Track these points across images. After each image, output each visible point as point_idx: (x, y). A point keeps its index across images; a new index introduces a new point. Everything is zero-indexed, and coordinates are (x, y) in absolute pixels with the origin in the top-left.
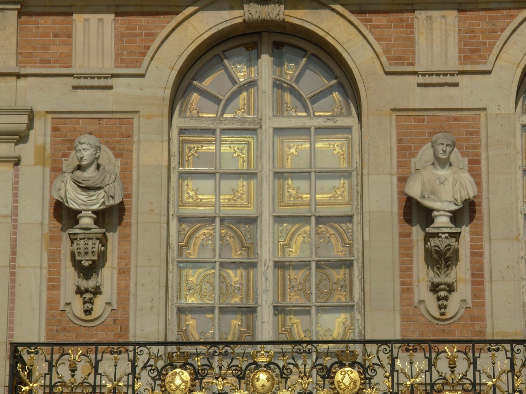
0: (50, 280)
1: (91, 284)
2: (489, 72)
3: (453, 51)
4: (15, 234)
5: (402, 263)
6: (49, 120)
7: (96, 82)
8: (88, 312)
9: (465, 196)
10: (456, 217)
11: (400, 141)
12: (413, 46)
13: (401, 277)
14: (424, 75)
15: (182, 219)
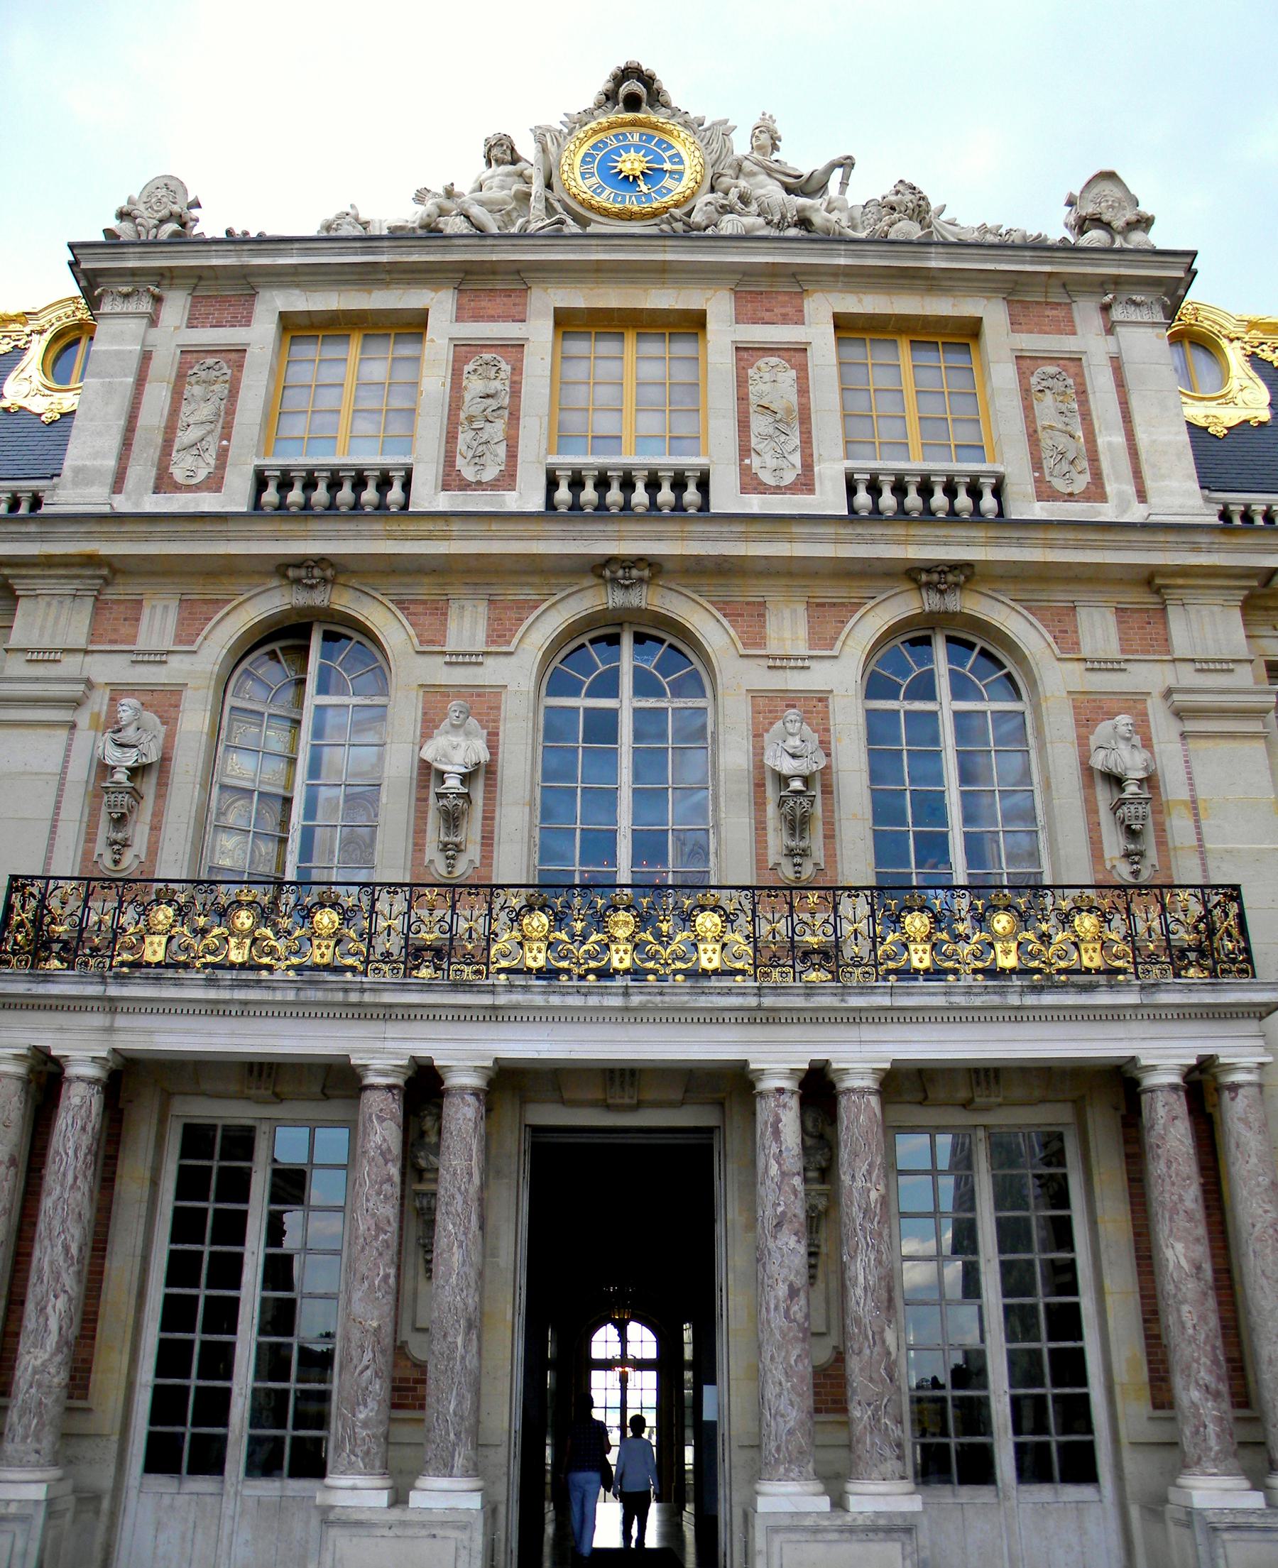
0: (88, 833)
1: (120, 836)
2: (510, 654)
3: (481, 635)
4: (62, 790)
5: (416, 825)
6: (108, 692)
7: (152, 658)
8: (116, 862)
9: (474, 760)
10: (466, 778)
11: (425, 714)
12: (445, 631)
13: (414, 838)
14: (451, 655)
15: (223, 787)
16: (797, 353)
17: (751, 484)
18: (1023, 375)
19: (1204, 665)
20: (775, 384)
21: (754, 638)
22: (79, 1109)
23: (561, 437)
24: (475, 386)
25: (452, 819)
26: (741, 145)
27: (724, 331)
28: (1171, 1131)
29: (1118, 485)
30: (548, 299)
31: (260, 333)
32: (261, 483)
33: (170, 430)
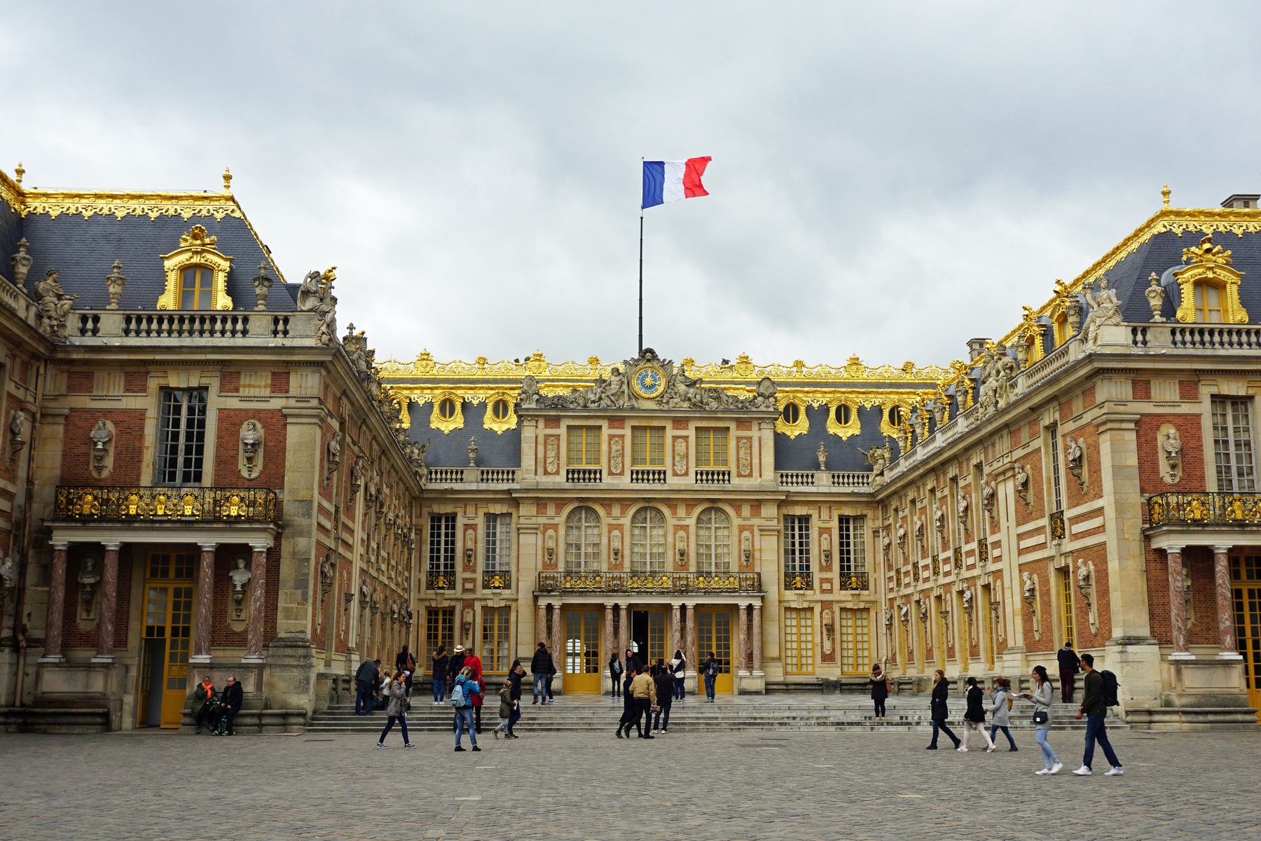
16: (686, 438)
17: (675, 474)
18: (738, 442)
19: (768, 519)
21: (674, 513)
22: (557, 613)
23: (634, 461)
24: (614, 448)
25: (616, 554)
26: (675, 372)
27: (670, 432)
28: (743, 616)
29: (756, 473)
30: (629, 424)
31: (562, 431)
32: (568, 472)
33: (545, 457)
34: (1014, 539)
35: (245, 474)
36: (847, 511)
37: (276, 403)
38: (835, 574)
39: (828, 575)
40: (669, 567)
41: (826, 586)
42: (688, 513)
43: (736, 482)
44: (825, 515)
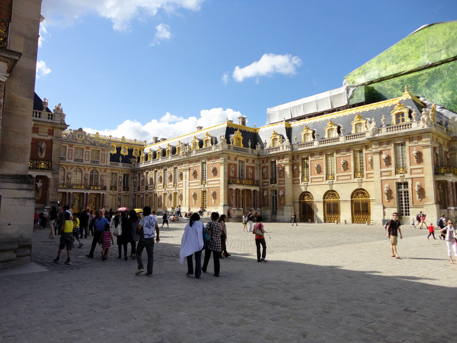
16: (89, 152)
20: (87, 153)
21: (85, 170)
28: (102, 196)
29: (105, 162)
30: (74, 146)
34: (187, 184)
35: (40, 156)
36: (125, 173)
37: (50, 138)
38: (122, 187)
39: (120, 187)
40: (83, 183)
41: (120, 190)
42: (89, 170)
43: (100, 163)
44: (120, 173)
